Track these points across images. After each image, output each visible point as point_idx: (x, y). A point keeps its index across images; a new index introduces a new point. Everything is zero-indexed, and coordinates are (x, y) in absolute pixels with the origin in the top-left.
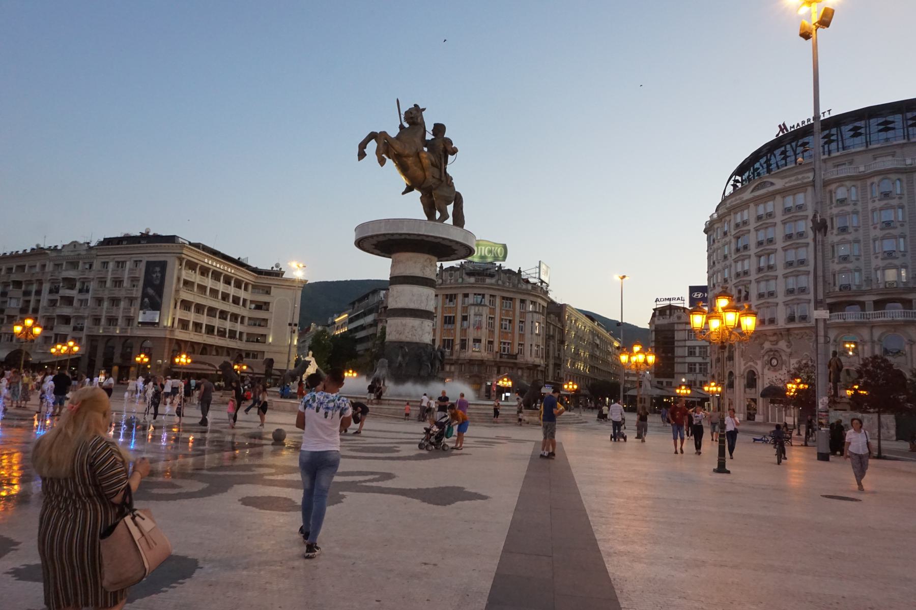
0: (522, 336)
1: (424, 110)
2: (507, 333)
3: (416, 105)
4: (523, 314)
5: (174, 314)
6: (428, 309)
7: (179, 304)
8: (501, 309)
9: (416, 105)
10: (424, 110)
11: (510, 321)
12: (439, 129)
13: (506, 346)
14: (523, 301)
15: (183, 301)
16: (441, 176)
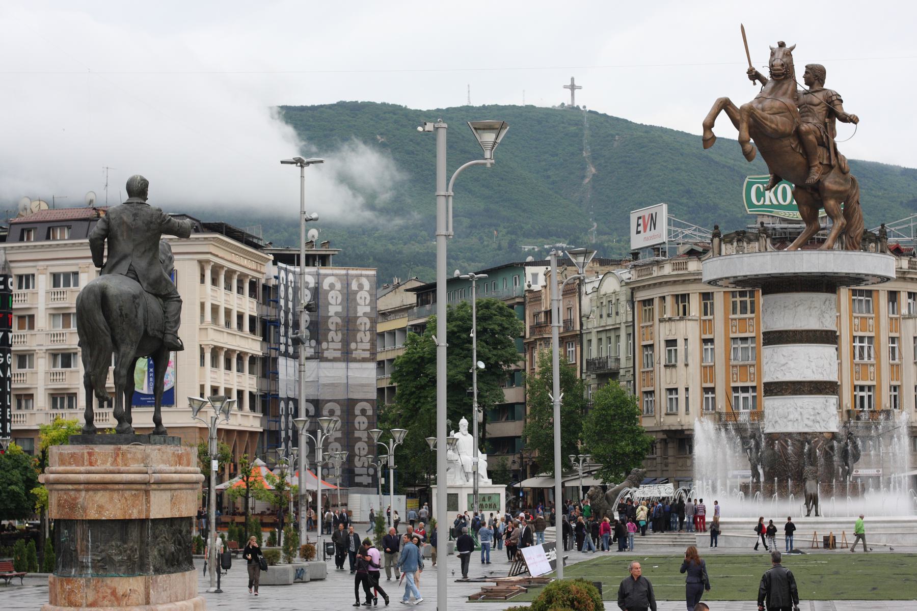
0: (896, 369)
1: (792, 49)
2: (867, 365)
3: (782, 45)
4: (894, 323)
5: (202, 376)
6: (834, 378)
7: (208, 356)
8: (851, 316)
9: (782, 45)
10: (792, 49)
11: (870, 339)
12: (816, 75)
13: (865, 394)
14: (893, 296)
15: (215, 351)
16: (829, 158)
